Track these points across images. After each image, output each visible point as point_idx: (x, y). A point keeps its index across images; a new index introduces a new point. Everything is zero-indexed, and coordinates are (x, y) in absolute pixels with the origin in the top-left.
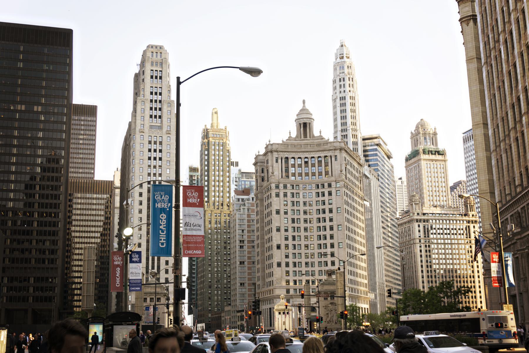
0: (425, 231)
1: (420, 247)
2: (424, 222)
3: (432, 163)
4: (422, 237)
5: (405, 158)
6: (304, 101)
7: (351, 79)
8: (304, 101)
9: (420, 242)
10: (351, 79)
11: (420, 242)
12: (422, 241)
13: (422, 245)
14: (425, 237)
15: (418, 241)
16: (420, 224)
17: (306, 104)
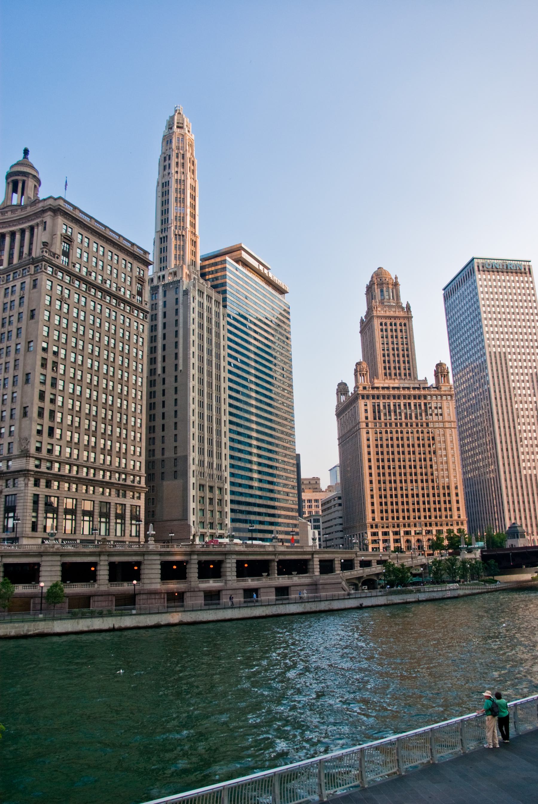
0: (374, 412)
1: (368, 433)
2: (373, 398)
3: (388, 322)
4: (369, 419)
5: (359, 321)
6: (26, 152)
7: (180, 156)
8: (26, 152)
9: (367, 425)
10: (180, 156)
11: (367, 425)
12: (370, 425)
13: (370, 430)
14: (375, 419)
15: (363, 425)
16: (367, 401)
17: (29, 157)
